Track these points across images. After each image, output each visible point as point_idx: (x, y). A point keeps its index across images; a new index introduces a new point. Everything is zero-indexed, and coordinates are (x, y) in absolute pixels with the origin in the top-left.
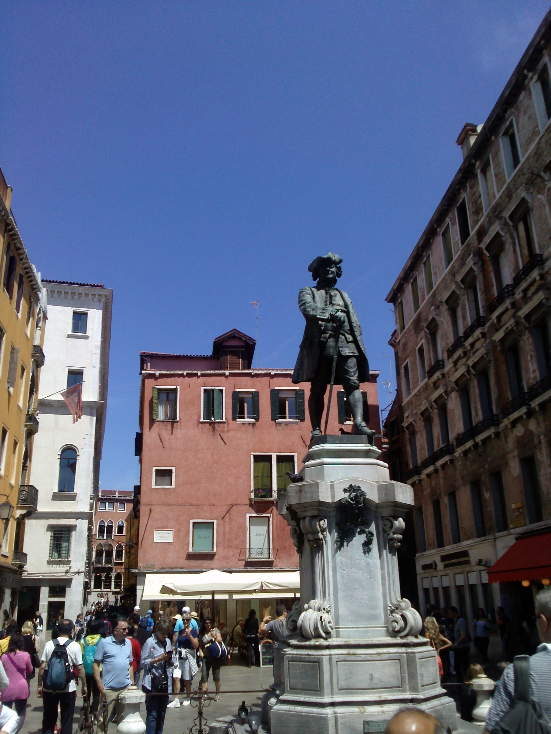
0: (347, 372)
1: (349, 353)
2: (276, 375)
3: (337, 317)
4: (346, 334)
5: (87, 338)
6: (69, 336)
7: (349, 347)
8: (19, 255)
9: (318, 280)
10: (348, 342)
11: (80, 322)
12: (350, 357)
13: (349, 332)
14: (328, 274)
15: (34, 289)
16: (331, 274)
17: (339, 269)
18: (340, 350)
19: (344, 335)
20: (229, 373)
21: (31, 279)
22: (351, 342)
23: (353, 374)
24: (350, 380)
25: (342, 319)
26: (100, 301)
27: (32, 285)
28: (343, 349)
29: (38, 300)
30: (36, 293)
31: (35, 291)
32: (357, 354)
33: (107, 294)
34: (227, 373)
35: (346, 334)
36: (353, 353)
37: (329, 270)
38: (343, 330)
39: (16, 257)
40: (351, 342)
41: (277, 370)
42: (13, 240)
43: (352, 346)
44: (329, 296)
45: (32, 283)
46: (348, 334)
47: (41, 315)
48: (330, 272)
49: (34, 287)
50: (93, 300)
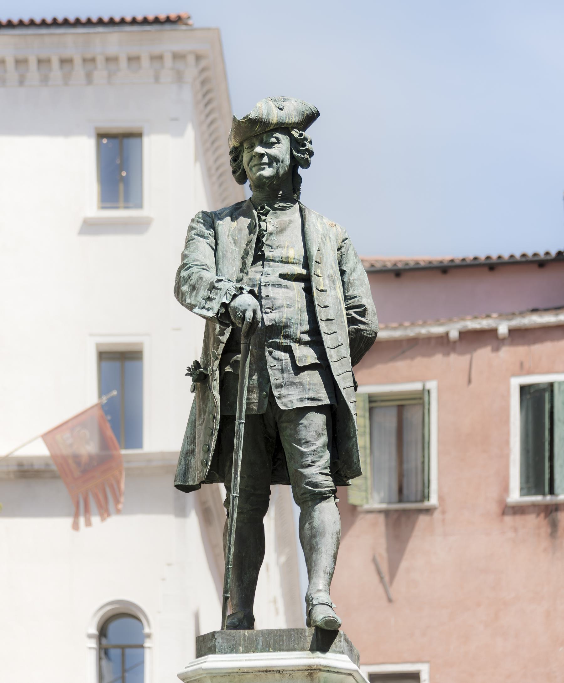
1: (301, 400)
11: (118, 156)
12: (303, 411)
13: (306, 338)
16: (270, 165)
17: (297, 144)
19: (288, 350)
22: (312, 367)
25: (249, 315)
28: (284, 391)
32: (327, 401)
35: (295, 346)
38: (287, 337)
40: (312, 367)
44: (254, 237)
48: (265, 160)
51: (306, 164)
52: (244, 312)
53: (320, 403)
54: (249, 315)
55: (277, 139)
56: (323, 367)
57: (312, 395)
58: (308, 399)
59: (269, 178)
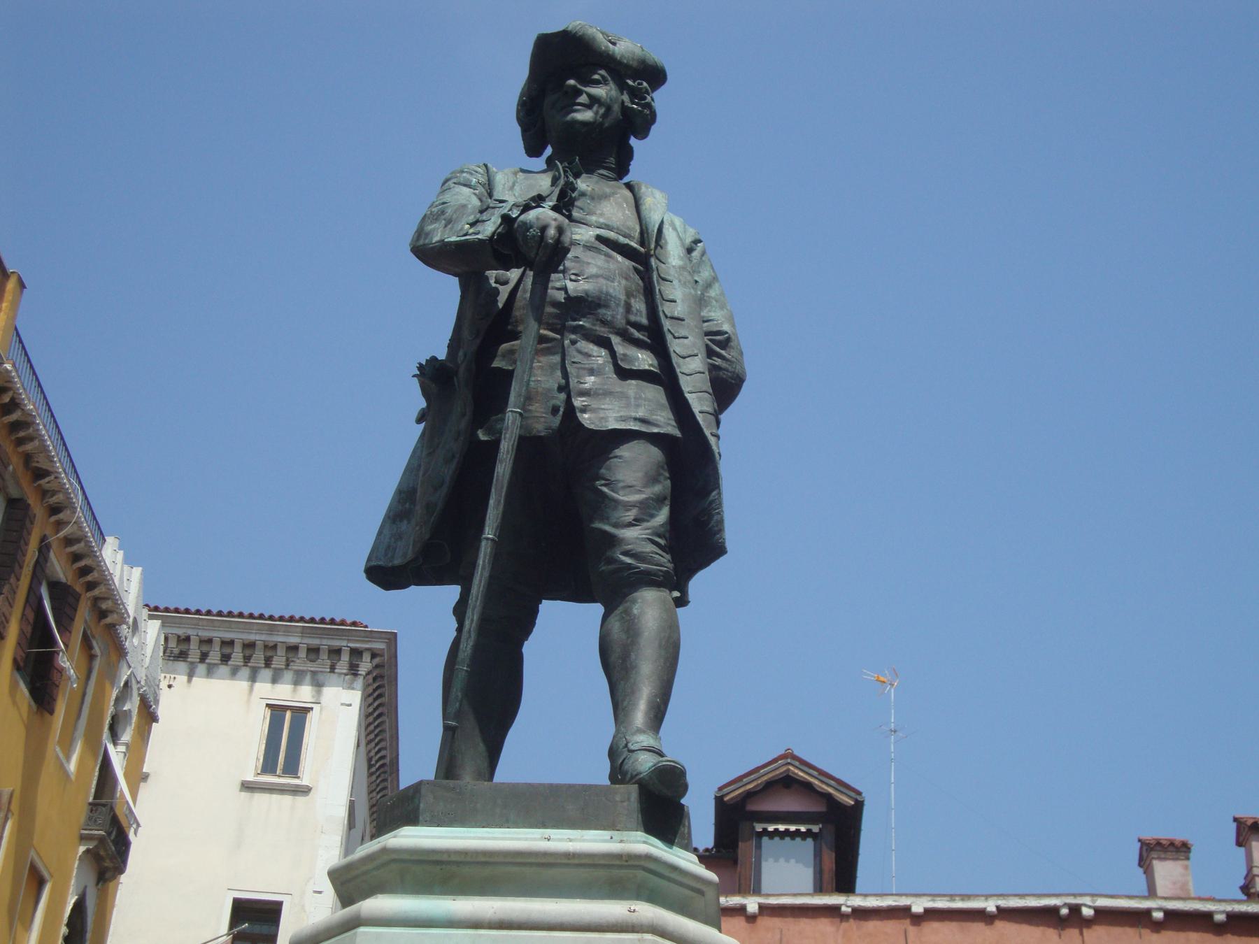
0: (602, 505)
2: (931, 914)
3: (527, 226)
4: (615, 340)
5: (304, 791)
6: (247, 787)
7: (623, 396)
8: (44, 493)
9: (549, 151)
10: (625, 374)
11: (284, 742)
14: (570, 106)
15: (103, 614)
16: (589, 107)
18: (578, 402)
19: (605, 343)
20: (761, 907)
21: (89, 578)
23: (631, 515)
24: (612, 541)
25: (552, 232)
26: (353, 669)
27: (96, 600)
28: (593, 403)
29: (120, 652)
30: (112, 628)
31: (109, 620)
33: (379, 646)
34: (752, 904)
35: (615, 340)
36: (643, 421)
37: (579, 93)
39: (32, 500)
41: (934, 896)
42: (20, 442)
43: (654, 394)
45: (96, 592)
46: (638, 344)
47: (132, 705)
48: (583, 99)
49: (104, 606)
50: (333, 669)
51: (643, 133)
52: (544, 229)
53: (656, 430)
54: (552, 232)
55: (603, 76)
56: (666, 378)
57: (641, 413)
58: (636, 419)
59: (584, 124)
